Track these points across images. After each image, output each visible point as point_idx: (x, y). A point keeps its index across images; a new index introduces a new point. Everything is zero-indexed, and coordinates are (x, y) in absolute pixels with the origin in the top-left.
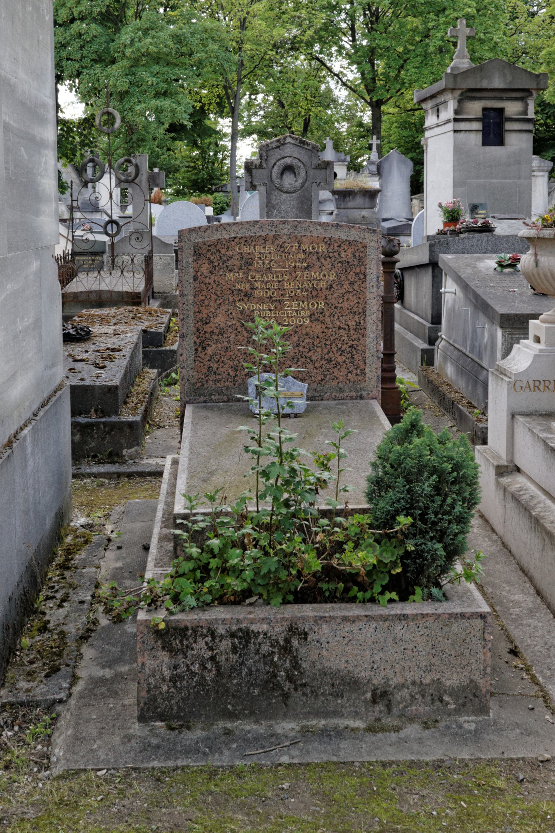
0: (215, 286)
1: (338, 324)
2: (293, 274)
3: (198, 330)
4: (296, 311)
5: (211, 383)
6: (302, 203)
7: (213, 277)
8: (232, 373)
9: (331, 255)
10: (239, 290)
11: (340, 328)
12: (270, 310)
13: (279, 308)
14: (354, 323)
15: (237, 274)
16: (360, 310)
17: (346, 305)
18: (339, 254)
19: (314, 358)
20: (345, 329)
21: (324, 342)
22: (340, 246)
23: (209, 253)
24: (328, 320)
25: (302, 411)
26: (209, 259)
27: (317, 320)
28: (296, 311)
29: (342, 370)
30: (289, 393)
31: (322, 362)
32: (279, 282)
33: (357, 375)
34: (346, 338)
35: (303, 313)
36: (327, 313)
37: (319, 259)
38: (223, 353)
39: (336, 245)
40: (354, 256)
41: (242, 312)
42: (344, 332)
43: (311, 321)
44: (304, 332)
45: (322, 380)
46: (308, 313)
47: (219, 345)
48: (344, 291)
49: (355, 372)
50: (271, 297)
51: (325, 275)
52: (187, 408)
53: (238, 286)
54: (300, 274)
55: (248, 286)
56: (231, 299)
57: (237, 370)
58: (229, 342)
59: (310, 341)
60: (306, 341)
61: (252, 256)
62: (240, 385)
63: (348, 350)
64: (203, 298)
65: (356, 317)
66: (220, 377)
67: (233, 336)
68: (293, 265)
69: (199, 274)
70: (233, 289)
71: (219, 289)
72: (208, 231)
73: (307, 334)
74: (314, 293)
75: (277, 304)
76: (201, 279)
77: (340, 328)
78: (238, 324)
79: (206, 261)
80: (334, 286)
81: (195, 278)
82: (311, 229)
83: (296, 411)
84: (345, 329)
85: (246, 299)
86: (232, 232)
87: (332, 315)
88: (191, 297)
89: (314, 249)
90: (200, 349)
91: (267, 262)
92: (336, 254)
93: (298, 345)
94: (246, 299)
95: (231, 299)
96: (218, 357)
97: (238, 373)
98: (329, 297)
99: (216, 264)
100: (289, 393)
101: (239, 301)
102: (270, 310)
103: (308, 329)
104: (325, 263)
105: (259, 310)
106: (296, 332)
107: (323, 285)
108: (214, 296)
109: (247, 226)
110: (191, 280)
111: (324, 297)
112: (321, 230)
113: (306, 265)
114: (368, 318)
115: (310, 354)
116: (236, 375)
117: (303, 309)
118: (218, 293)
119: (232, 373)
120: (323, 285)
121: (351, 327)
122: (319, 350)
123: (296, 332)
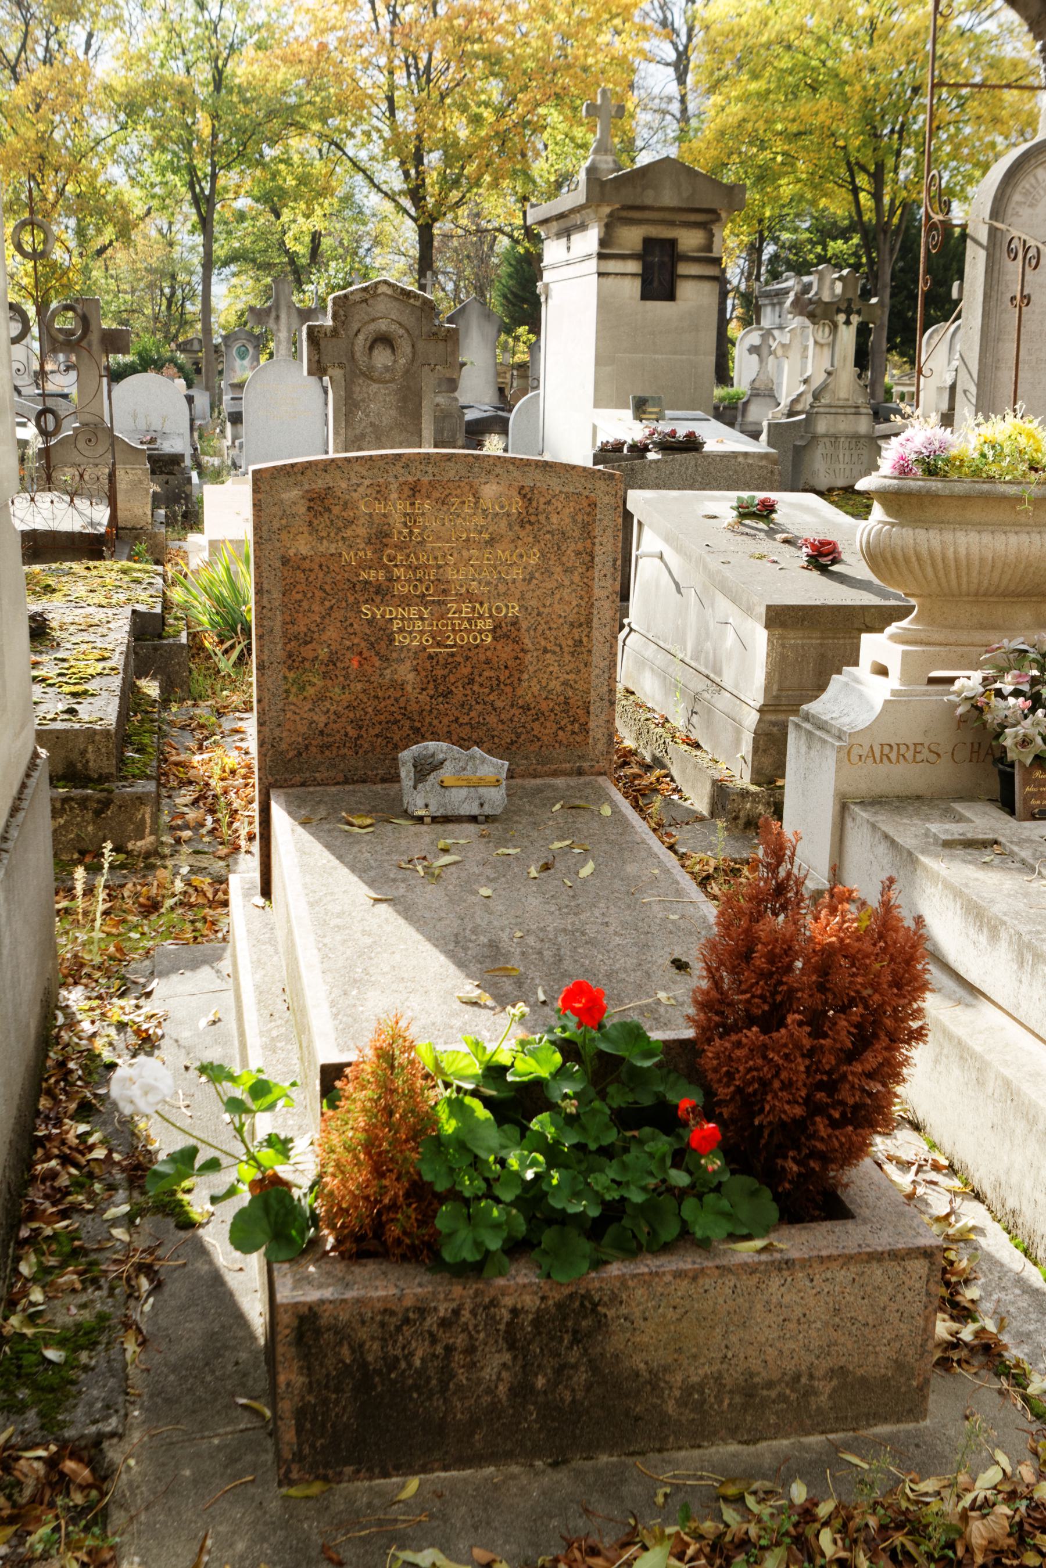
3: (290, 656)
4: (469, 620)
6: (404, 399)
8: (353, 733)
9: (533, 519)
10: (366, 582)
11: (545, 651)
12: (422, 619)
14: (570, 642)
15: (361, 554)
19: (499, 704)
22: (549, 503)
25: (498, 811)
31: (513, 711)
32: (439, 567)
36: (524, 625)
37: (510, 526)
39: (542, 500)
40: (575, 521)
41: (371, 622)
44: (482, 658)
45: (512, 743)
46: (489, 624)
53: (364, 575)
55: (381, 575)
56: (351, 599)
59: (492, 674)
60: (486, 674)
62: (366, 753)
64: (299, 596)
67: (355, 664)
72: (309, 472)
73: (488, 662)
75: (436, 608)
77: (545, 651)
78: (363, 644)
83: (487, 810)
86: (352, 475)
88: (276, 595)
89: (502, 507)
93: (472, 681)
95: (351, 599)
97: (363, 732)
99: (324, 534)
101: (366, 602)
102: (422, 619)
104: (522, 534)
105: (403, 619)
106: (467, 658)
108: (319, 594)
109: (381, 463)
110: (278, 564)
111: (518, 595)
112: (516, 474)
113: (487, 536)
114: (595, 634)
116: (360, 737)
118: (327, 588)
119: (353, 733)
120: (516, 574)
122: (508, 689)
123: (467, 658)
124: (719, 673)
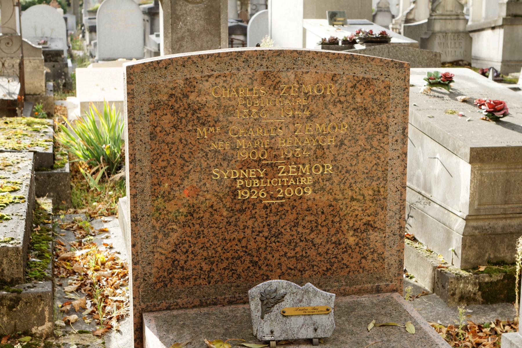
0: (181, 147)
1: (350, 193)
2: (291, 127)
3: (158, 210)
4: (295, 178)
5: (176, 281)
6: (209, 14)
7: (178, 134)
8: (206, 267)
9: (342, 99)
10: (216, 151)
11: (353, 199)
12: (259, 178)
13: (270, 175)
14: (371, 192)
15: (212, 129)
16: (380, 174)
17: (361, 167)
18: (353, 98)
19: (317, 241)
20: (358, 201)
21: (331, 218)
22: (354, 87)
23: (173, 100)
24: (336, 188)
25: (329, 334)
26: (172, 107)
27: (323, 189)
28: (295, 178)
29: (354, 255)
30: (309, 309)
31: (328, 246)
32: (272, 138)
33: (373, 260)
34: (360, 213)
35: (303, 181)
36: (336, 180)
37: (326, 105)
38: (194, 241)
39: (350, 85)
40: (374, 100)
41: (219, 182)
42: (358, 204)
43: (314, 191)
44: (305, 206)
45: (327, 270)
46: (310, 180)
47: (188, 230)
48: (359, 149)
49: (370, 257)
50: (260, 160)
51: (334, 128)
52: (144, 317)
53: (214, 146)
54: (300, 126)
55: (227, 146)
56: (204, 165)
57: (212, 263)
58: (201, 225)
59: (312, 218)
60: (307, 218)
61: (233, 103)
62: (216, 282)
63: (363, 228)
64: (164, 164)
65: (374, 183)
66: (189, 273)
67: (207, 215)
68: (291, 113)
69: (158, 129)
70: (207, 150)
71: (187, 150)
72: (171, 67)
73: (308, 209)
74: (319, 153)
75: (269, 169)
76: (160, 136)
77: (353, 199)
78: (214, 199)
79: (168, 112)
80: (346, 142)
81: (153, 136)
82: (316, 63)
83: (320, 334)
84: (358, 201)
85: (225, 164)
86: (205, 69)
87: (343, 182)
88: (146, 163)
89: (319, 91)
90: (160, 236)
91: (254, 110)
92: (349, 98)
93: (296, 225)
94: (225, 164)
95: (204, 165)
96: (186, 246)
97: (214, 267)
98: (339, 157)
99: (183, 115)
100: (309, 309)
101: (216, 166)
102: (259, 178)
103: (309, 203)
104: (335, 111)
105: (244, 179)
106: (293, 207)
107: (330, 141)
108: (179, 161)
109: (227, 59)
110: (147, 139)
111: (332, 158)
112: (330, 65)
113: (308, 113)
114: (390, 185)
115: (312, 236)
116: (212, 270)
117: (303, 175)
118: (186, 156)
119: (206, 267)
120: (330, 141)
121: (368, 198)
122: (324, 230)
123: (293, 207)
124: (430, 192)
